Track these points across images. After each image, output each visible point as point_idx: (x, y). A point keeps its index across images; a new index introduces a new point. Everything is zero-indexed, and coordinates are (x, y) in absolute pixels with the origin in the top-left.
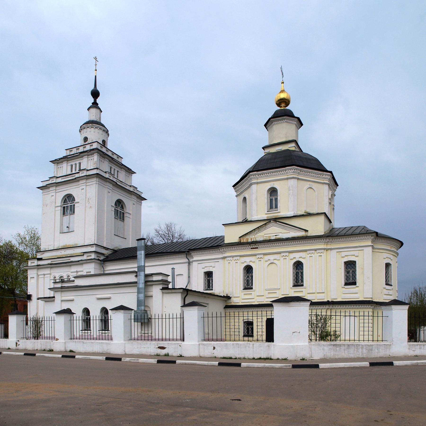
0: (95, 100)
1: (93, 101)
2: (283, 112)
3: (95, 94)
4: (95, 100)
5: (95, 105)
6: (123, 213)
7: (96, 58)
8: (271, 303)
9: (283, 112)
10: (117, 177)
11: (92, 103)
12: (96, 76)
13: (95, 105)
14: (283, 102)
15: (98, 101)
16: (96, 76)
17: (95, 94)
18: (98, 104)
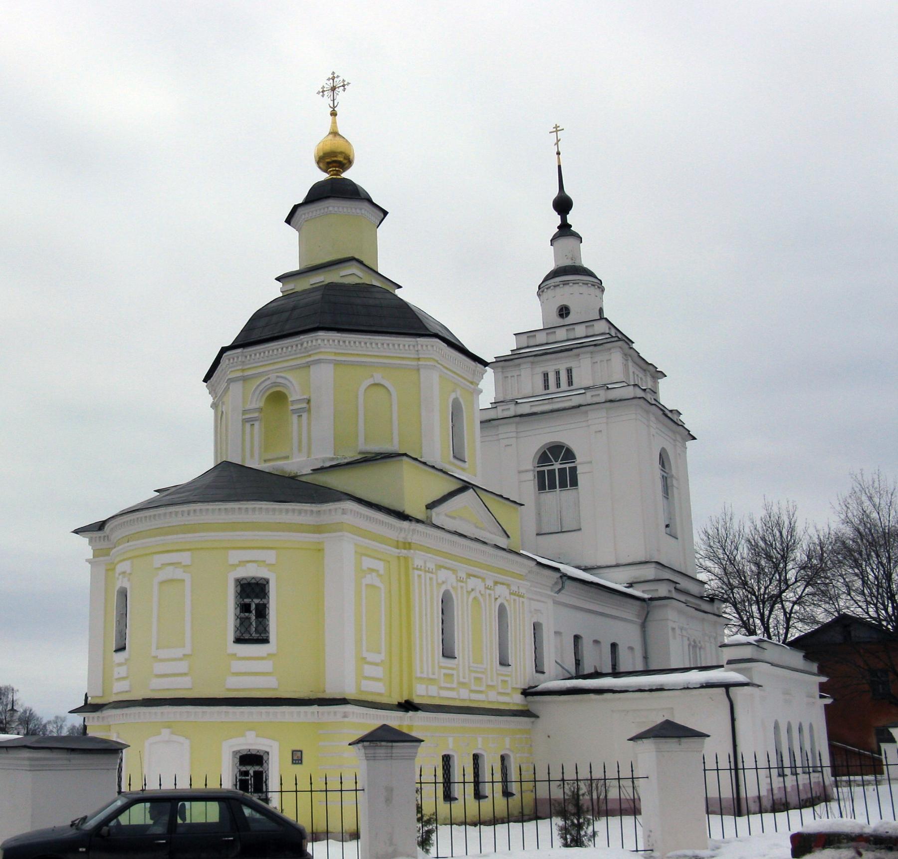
0: (564, 219)
1: (559, 222)
2: (335, 187)
3: (563, 205)
4: (564, 219)
5: (565, 229)
6: (574, 470)
7: (557, 129)
8: (77, 720)
9: (335, 187)
10: (570, 383)
11: (559, 227)
12: (559, 167)
13: (565, 229)
14: (335, 160)
15: (570, 219)
16: (559, 167)
17: (563, 205)
18: (571, 226)
